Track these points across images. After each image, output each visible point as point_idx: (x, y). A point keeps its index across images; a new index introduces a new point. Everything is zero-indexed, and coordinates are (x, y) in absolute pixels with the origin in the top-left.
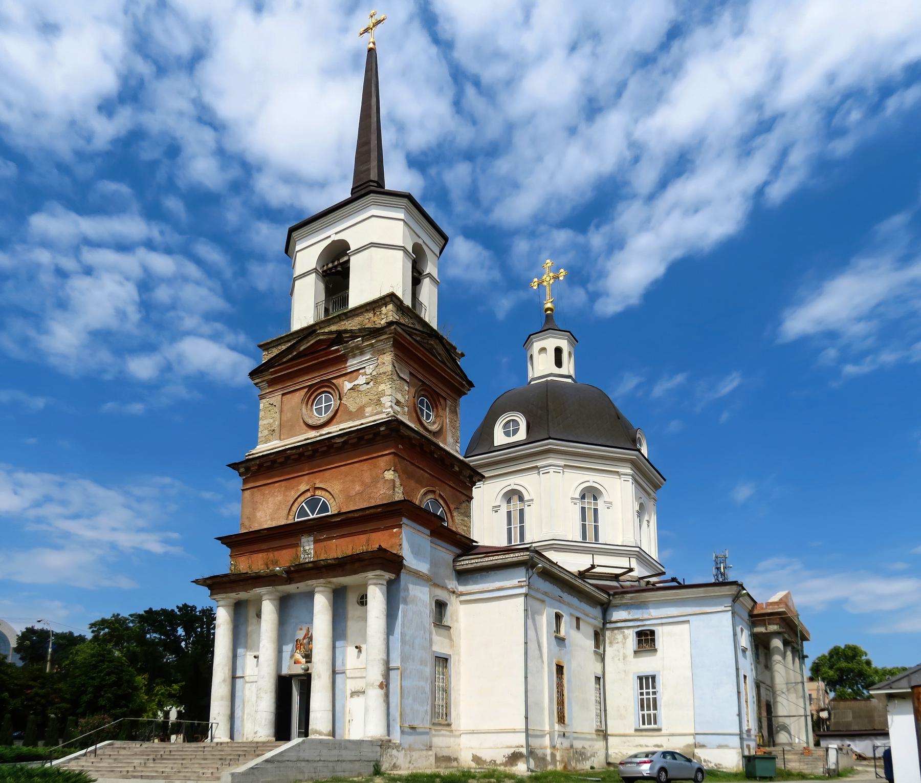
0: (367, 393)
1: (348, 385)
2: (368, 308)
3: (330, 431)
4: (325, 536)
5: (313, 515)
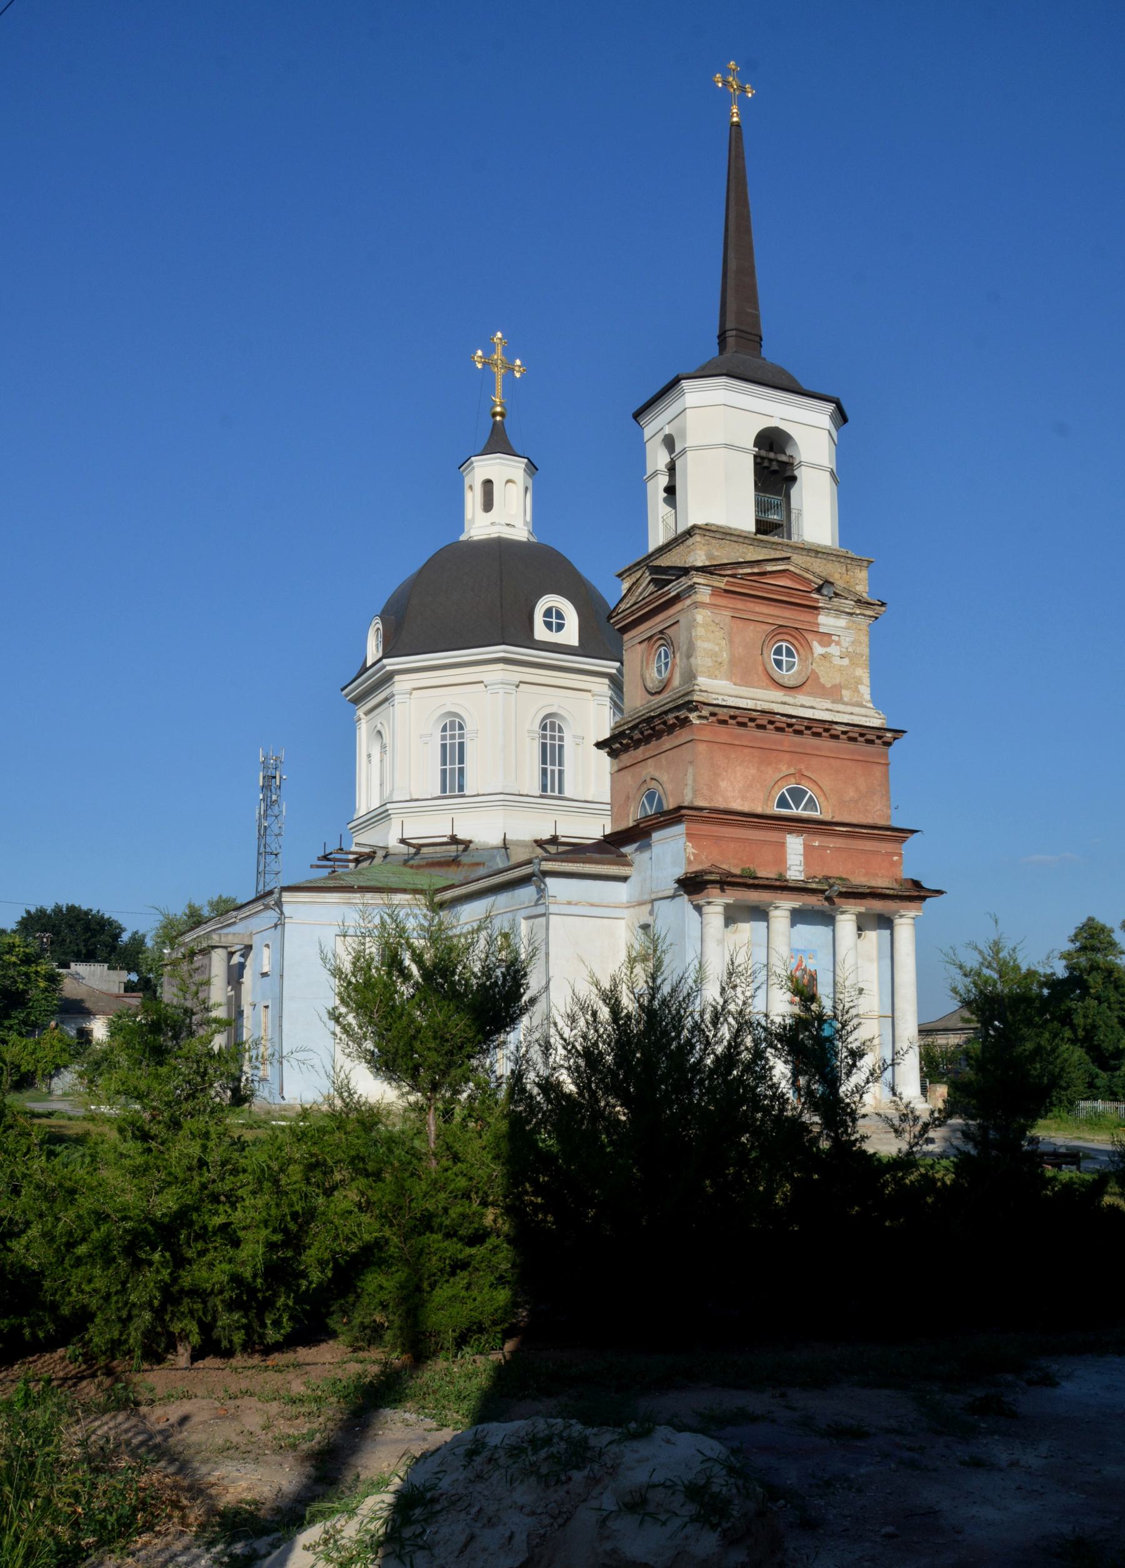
0: (841, 669)
1: (818, 649)
2: (842, 560)
3: (814, 705)
4: (817, 844)
5: (797, 809)
